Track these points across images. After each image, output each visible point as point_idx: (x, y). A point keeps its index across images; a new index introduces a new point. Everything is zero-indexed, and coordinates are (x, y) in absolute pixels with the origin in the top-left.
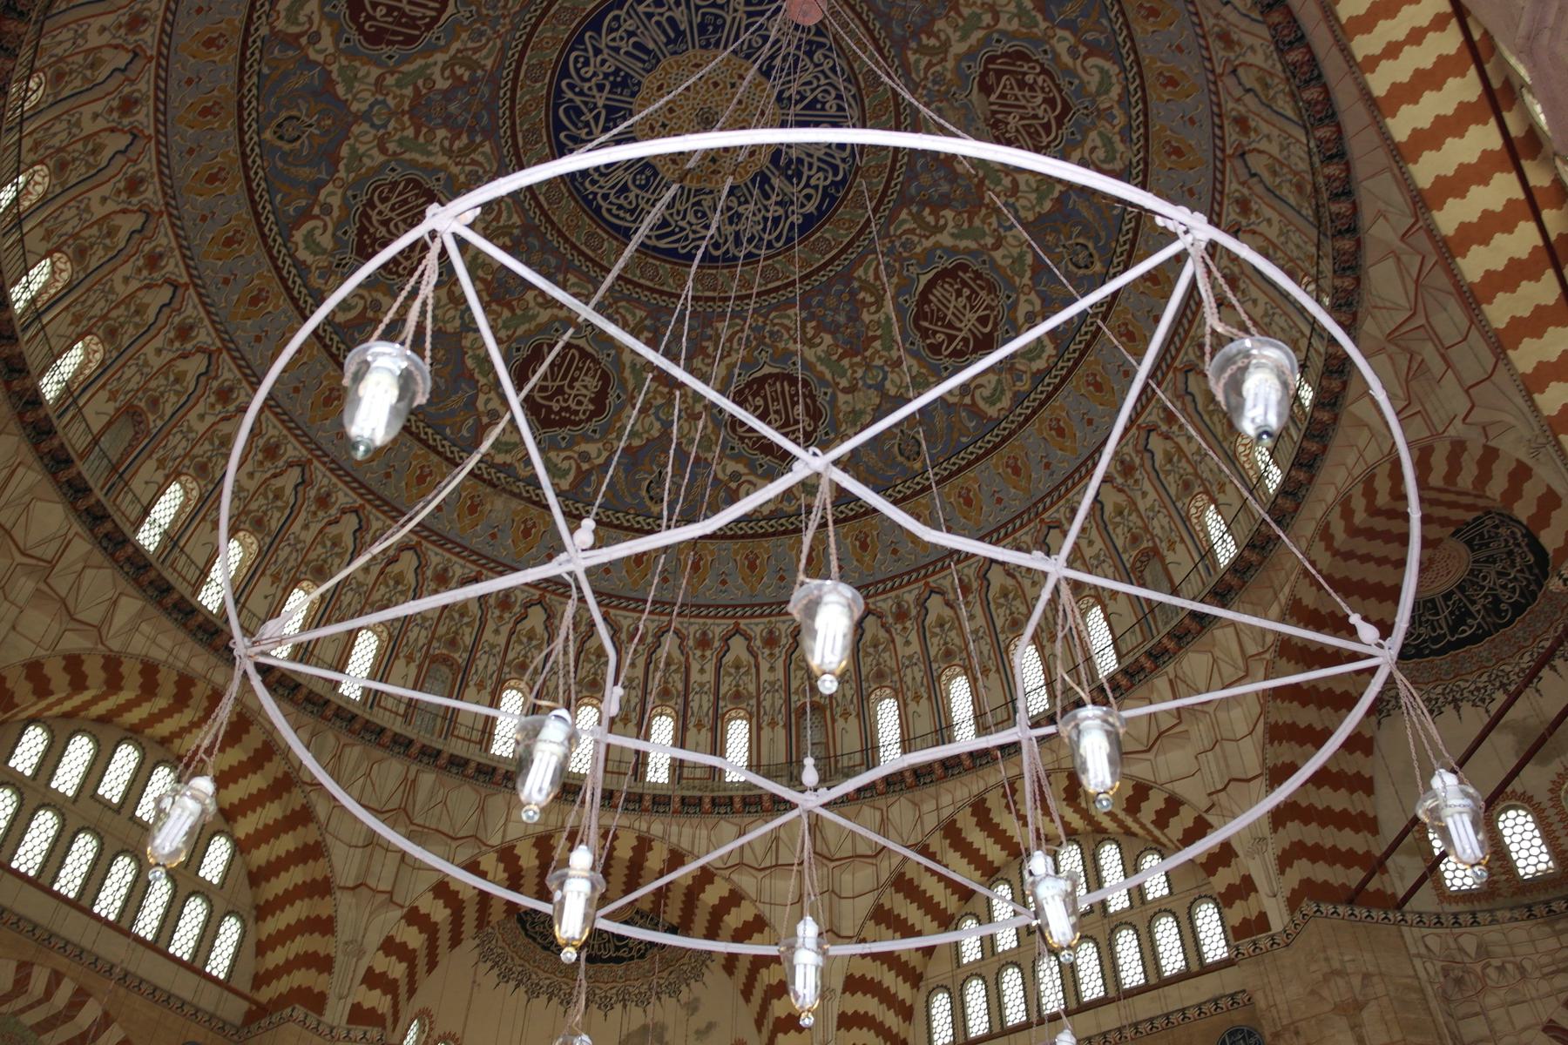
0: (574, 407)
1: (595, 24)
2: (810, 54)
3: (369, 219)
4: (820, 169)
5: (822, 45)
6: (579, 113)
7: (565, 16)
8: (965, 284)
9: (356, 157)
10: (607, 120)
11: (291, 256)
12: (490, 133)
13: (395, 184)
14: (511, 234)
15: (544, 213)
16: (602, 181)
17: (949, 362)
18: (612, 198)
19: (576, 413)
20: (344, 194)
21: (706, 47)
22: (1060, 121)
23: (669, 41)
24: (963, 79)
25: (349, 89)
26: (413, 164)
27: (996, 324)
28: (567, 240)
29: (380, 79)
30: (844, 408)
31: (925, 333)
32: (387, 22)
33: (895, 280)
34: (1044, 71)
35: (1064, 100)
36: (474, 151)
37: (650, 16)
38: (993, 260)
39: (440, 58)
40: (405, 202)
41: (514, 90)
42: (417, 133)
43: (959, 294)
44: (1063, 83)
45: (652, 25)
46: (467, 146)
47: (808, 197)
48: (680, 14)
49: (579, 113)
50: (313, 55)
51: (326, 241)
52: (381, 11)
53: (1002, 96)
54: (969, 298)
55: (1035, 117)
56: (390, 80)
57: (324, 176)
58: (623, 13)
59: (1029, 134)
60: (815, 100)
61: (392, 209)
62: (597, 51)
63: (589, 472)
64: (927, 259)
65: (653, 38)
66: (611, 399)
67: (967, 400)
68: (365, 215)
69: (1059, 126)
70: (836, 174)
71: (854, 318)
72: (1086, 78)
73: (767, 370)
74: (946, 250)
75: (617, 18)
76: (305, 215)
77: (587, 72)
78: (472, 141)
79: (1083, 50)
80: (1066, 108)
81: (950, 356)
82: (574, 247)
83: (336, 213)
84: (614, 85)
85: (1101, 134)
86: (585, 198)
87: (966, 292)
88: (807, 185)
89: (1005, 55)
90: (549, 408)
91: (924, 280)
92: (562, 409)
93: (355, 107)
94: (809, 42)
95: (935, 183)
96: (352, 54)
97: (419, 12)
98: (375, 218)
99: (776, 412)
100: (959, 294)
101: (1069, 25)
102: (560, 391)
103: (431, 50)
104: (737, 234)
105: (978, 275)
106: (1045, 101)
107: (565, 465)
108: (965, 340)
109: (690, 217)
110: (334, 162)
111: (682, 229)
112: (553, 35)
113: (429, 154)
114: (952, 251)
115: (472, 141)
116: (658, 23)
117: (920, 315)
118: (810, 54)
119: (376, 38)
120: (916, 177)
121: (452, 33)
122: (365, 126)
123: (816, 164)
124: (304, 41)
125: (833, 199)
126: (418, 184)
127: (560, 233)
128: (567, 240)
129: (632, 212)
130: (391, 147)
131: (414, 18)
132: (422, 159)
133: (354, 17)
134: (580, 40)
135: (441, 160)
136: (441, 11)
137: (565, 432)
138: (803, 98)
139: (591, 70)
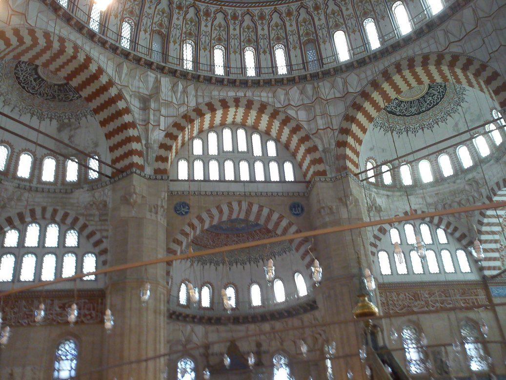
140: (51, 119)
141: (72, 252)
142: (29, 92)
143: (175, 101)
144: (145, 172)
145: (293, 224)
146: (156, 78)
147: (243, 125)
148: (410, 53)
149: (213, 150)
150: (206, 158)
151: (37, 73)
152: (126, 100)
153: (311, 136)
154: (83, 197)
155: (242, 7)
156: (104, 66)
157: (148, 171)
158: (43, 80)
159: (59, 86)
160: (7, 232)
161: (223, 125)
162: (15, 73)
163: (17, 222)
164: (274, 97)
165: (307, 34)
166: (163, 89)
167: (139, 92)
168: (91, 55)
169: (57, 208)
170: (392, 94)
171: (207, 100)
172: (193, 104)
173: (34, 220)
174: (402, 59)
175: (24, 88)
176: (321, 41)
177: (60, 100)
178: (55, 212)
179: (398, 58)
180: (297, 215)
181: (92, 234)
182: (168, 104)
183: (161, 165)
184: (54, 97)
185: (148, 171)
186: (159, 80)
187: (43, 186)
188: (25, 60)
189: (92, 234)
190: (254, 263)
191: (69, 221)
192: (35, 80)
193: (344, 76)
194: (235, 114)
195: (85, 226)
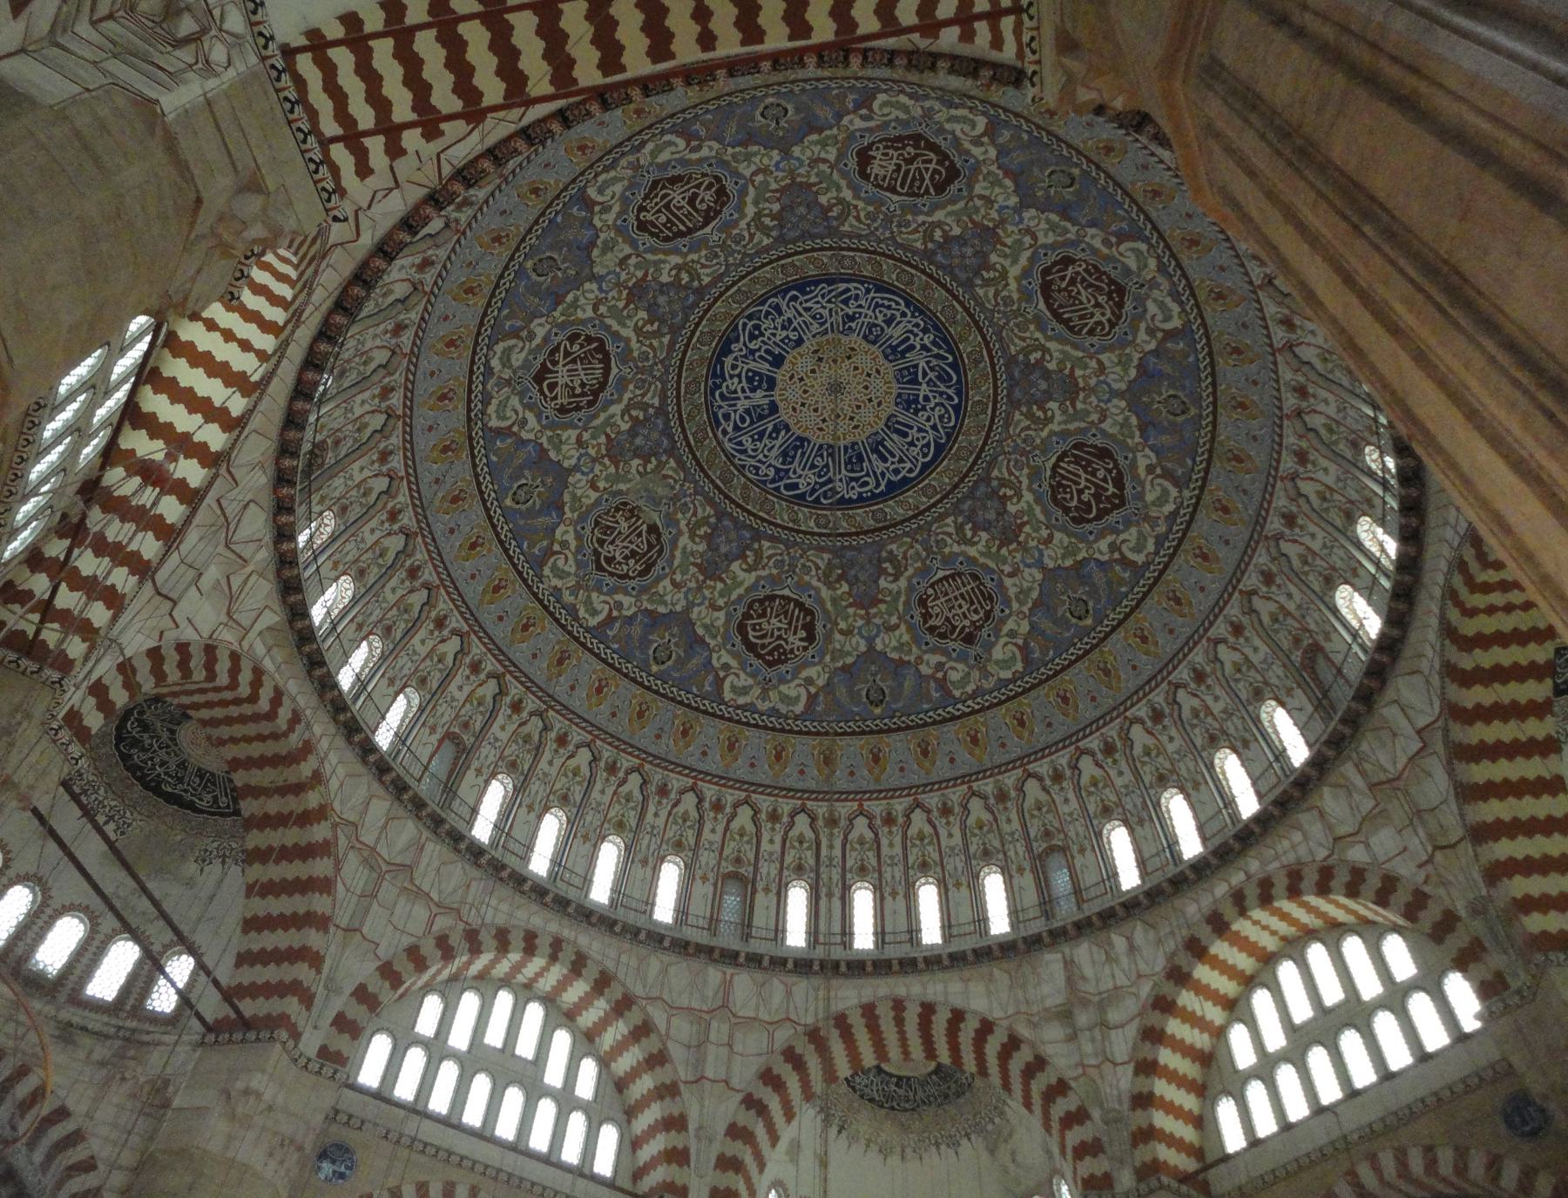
0: (891, 152)
1: (940, 448)
2: (778, 470)
3: (1113, 313)
4: (735, 392)
5: (773, 481)
6: (939, 377)
7: (964, 453)
8: (583, 394)
9: (1124, 363)
10: (916, 373)
11: (1184, 310)
12: (1011, 361)
13: (1091, 332)
14: (983, 279)
15: (956, 298)
16: (910, 327)
17: (559, 338)
18: (898, 314)
19: (886, 147)
20: (1135, 338)
21: (854, 444)
22: (597, 553)
23: (881, 443)
24: (671, 521)
25: (1127, 419)
26: (1076, 347)
27: (541, 391)
28: (931, 276)
29: (1103, 418)
30: (622, 246)
31: (589, 339)
32: (1097, 464)
33: (636, 354)
34: (625, 576)
35: (604, 570)
36: (1023, 349)
37: (901, 461)
38: (576, 427)
39: (1055, 427)
40: (1081, 317)
41: (996, 394)
42: (1072, 370)
43: (583, 385)
44: (611, 581)
45: (898, 453)
46: (1031, 352)
47: (734, 367)
48: (880, 466)
49: (939, 377)
50: (1152, 455)
51: (1152, 308)
52: (1101, 474)
53: (639, 535)
54: (573, 389)
55: (612, 542)
56: (1095, 417)
57: (1153, 360)
58: (922, 460)
59: (609, 527)
60: (760, 440)
61: (1092, 315)
62: (934, 427)
63: (857, 107)
64: (622, 383)
65: (894, 442)
66: (852, 163)
67: (524, 334)
68: (1119, 317)
69: (595, 550)
70: (722, 395)
71: (652, 308)
72: (602, 598)
73: (708, 230)
74: (612, 402)
75: (925, 455)
76: (1170, 335)
77: (938, 411)
78: (1026, 356)
79: (615, 613)
80: (600, 568)
81: (559, 344)
82: (923, 272)
83: (1143, 326)
84: (916, 401)
85: (569, 574)
86: (922, 312)
87: (579, 390)
88: (739, 376)
89: (654, 564)
90: (916, 147)
91: (614, 371)
92: (903, 148)
93: (1123, 404)
94: (781, 479)
95: (647, 438)
96: (1126, 447)
97: (1071, 468)
98: (1109, 314)
99: (679, 208)
100: (583, 385)
101: (630, 620)
102: (910, 161)
103: (1064, 434)
104: (780, 313)
105: (578, 408)
106: (614, 558)
107: (886, 111)
108: (555, 363)
109: (825, 313)
110: (1139, 367)
111: (829, 301)
112: (971, 438)
113: (1062, 352)
114: (605, 409)
115: (1026, 356)
116: (893, 456)
117: (601, 348)
118: (778, 470)
119: (1104, 454)
120: (663, 433)
121: (1045, 448)
122: (1115, 386)
123: (740, 394)
124: (1158, 471)
125: (715, 375)
126: (1071, 329)
127: (938, 282)
128: (931, 276)
129: (877, 305)
130: (1093, 364)
131: (1076, 463)
132: (1068, 348)
133: (1120, 473)
134: (948, 435)
135: (1052, 345)
136: (1055, 467)
137: (894, 133)
138: (770, 436)
139: (937, 413)
142: (906, 1110)
143: (1122, 980)
147: (1310, 935)
148: (1446, 551)
149: (1275, 1039)
150: (1265, 1069)
151: (891, 1075)
153: (1427, 889)
155: (1157, 686)
156: (959, 1003)
158: (908, 1079)
161: (1269, 960)
164: (1306, 838)
165: (1297, 641)
166: (1088, 971)
167: (1046, 1010)
168: (930, 998)
170: (1539, 653)
172: (1160, 964)
174: (1449, 573)
175: (892, 1108)
176: (1320, 638)
177: (958, 1095)
179: (1441, 579)
180: (1534, 1134)
182: (1115, 995)
183: (1143, 1154)
184: (946, 1096)
192: (897, 1085)
193: (1390, 694)
194: (1260, 927)
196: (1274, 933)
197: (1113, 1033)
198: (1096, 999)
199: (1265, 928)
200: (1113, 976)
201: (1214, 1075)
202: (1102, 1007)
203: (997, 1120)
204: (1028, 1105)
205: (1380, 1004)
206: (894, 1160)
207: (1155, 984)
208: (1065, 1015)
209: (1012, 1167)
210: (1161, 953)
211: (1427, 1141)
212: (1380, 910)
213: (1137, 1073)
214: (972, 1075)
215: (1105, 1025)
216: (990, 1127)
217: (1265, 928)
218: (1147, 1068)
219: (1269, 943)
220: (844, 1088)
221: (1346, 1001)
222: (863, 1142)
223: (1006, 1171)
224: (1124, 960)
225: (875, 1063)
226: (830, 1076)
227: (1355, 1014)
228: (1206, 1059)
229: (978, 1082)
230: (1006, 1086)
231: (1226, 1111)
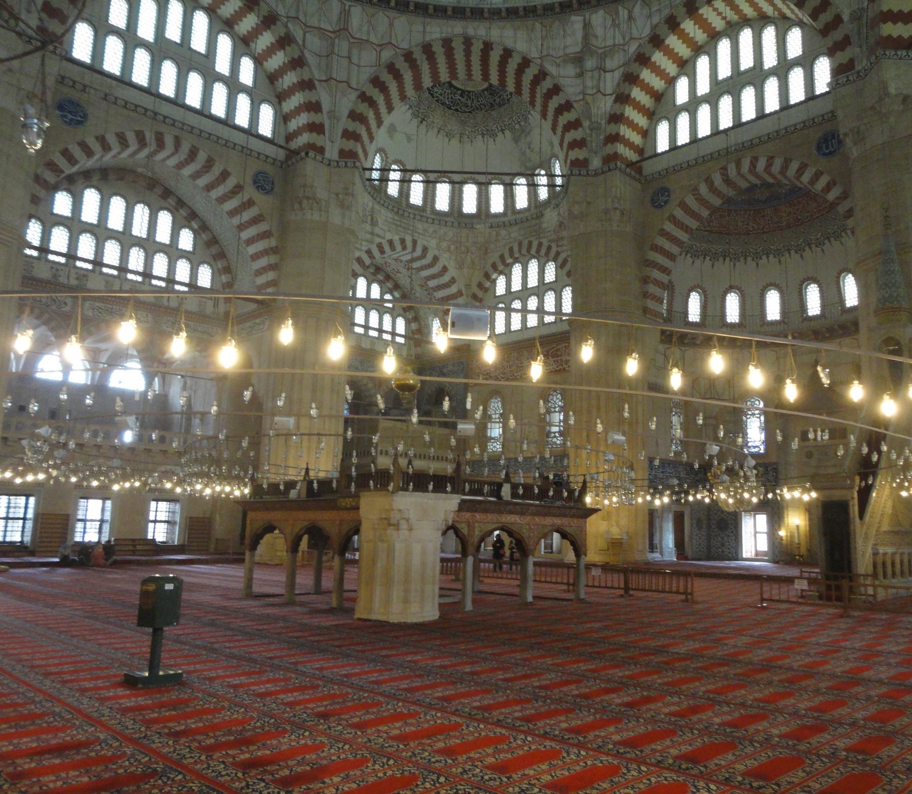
140: (502, 130)
141: (534, 294)
144: (591, 168)
145: (822, 173)
146: (584, 20)
147: (746, 22)
151: (458, 89)
152: (552, 76)
154: (551, 218)
157: (596, 163)
158: (469, 92)
159: (486, 89)
160: (496, 279)
162: (437, 101)
163: (501, 267)
166: (599, 32)
167: (566, 55)
169: (531, 239)
171: (666, 12)
172: (647, 32)
173: (516, 260)
175: (457, 110)
177: (500, 105)
178: (530, 243)
181: (565, 262)
183: (609, 149)
185: (596, 163)
186: (587, 22)
187: (522, 215)
188: (431, 84)
189: (565, 262)
190: (796, 252)
191: (543, 251)
192: (461, 95)
195: (558, 254)
196: (724, 18)
197: (607, 74)
198: (600, 51)
199: (719, 14)
200: (614, 37)
201: (662, 106)
202: (603, 56)
203: (523, 123)
204: (544, 116)
205: (773, 72)
206: (455, 142)
207: (640, 45)
208: (578, 60)
209: (528, 151)
210: (649, 23)
211: (770, 155)
212: (796, 10)
213: (616, 101)
214: (511, 94)
215: (602, 69)
216: (517, 127)
217: (719, 14)
218: (623, 98)
219: (718, 24)
220: (427, 94)
221: (754, 68)
222: (436, 130)
223: (524, 154)
224: (624, 27)
225: (448, 80)
226: (418, 86)
227: (756, 77)
228: (658, 97)
229: (515, 99)
230: (532, 102)
231: (663, 129)
